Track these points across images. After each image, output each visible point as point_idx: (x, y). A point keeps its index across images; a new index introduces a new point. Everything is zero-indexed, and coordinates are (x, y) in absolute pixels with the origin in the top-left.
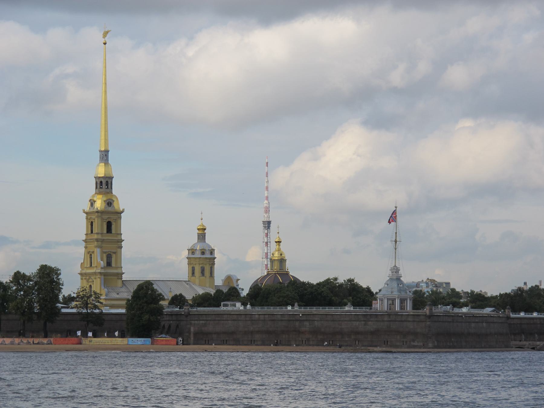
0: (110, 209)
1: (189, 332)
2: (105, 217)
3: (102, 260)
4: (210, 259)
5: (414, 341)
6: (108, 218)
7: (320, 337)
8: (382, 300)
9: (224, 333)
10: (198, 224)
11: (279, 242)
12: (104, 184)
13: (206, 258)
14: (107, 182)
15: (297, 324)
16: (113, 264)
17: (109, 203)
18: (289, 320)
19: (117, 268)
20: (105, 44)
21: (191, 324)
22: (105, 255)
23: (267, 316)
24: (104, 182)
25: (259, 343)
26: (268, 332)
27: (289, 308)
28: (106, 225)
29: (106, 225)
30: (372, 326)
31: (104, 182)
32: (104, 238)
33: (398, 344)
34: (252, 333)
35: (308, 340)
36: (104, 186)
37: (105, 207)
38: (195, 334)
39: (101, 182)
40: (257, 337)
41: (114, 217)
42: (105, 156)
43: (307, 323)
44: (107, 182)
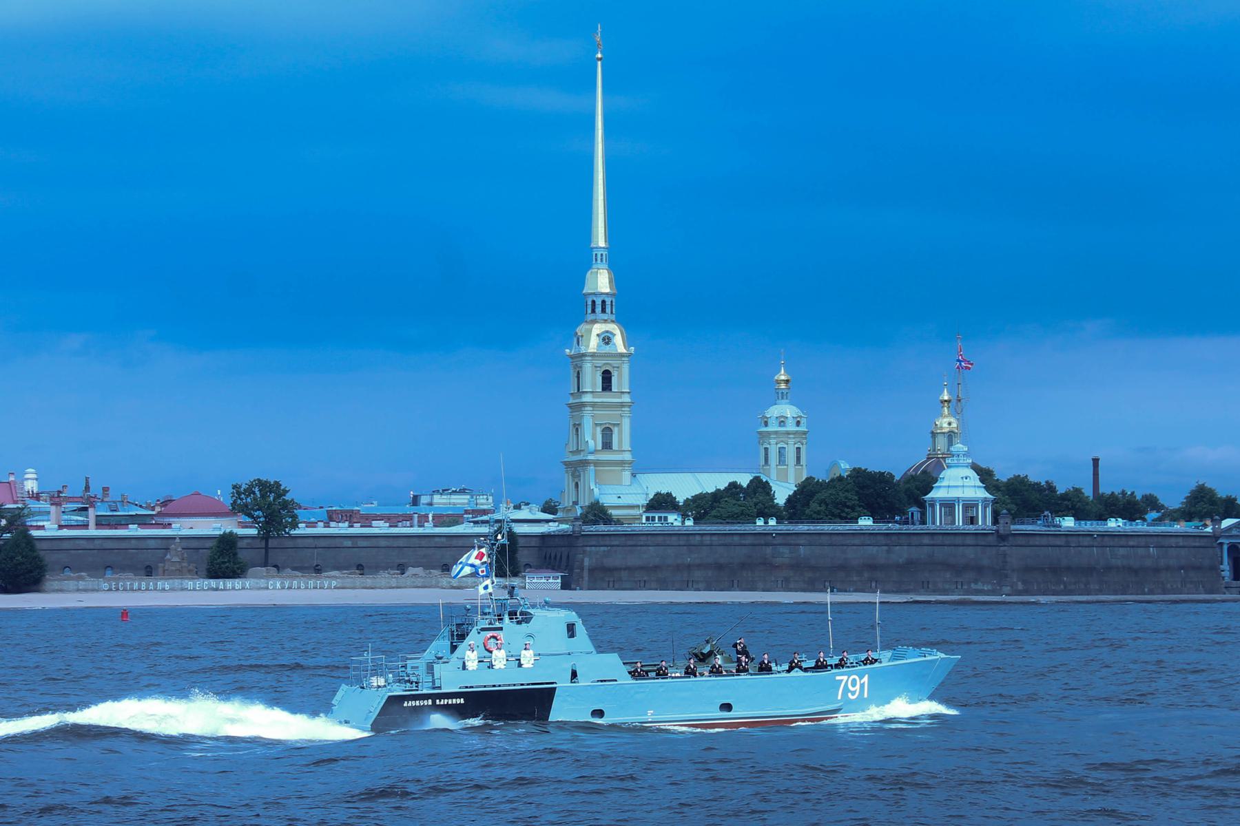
0: (607, 349)
1: (582, 569)
2: (600, 362)
3: (594, 438)
4: (795, 433)
5: (976, 582)
7: (808, 575)
8: (933, 506)
9: (642, 568)
11: (948, 401)
13: (788, 433)
14: (603, 302)
15: (769, 550)
16: (615, 447)
17: (607, 339)
18: (753, 545)
21: (584, 552)
22: (599, 430)
23: (714, 538)
24: (599, 302)
25: (700, 586)
26: (719, 567)
27: (760, 522)
30: (901, 554)
31: (599, 302)
33: (947, 586)
35: (787, 580)
36: (599, 309)
37: (599, 346)
39: (594, 302)
40: (698, 574)
41: (615, 363)
44: (603, 302)
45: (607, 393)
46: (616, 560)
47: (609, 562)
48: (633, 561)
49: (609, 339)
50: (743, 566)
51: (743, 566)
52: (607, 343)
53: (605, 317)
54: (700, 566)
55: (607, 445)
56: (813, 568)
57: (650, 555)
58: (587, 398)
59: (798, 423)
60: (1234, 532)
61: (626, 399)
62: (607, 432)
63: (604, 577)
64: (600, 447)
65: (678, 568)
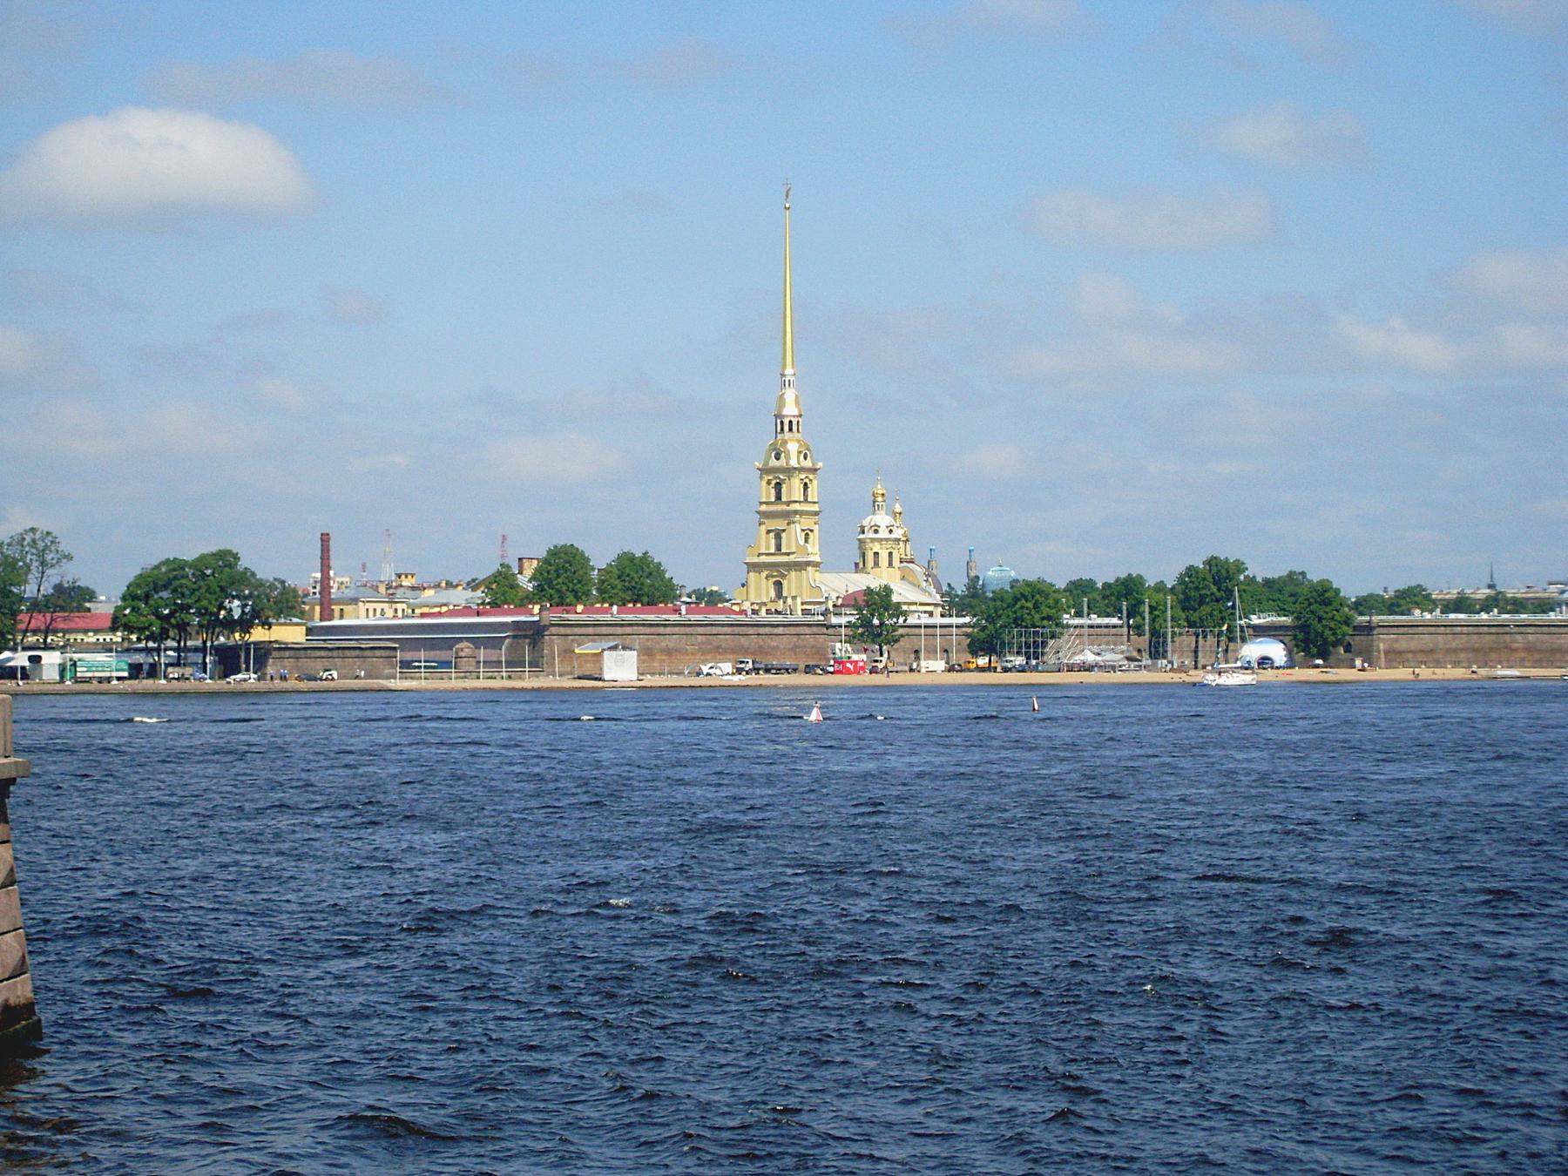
2: (803, 476)
7: (1537, 656)
9: (1422, 651)
26: (1475, 650)
34: (1455, 651)
35: (1523, 659)
38: (1387, 652)
40: (1462, 656)
43: (1519, 637)
46: (1404, 643)
47: (1396, 646)
48: (1413, 645)
50: (1491, 650)
51: (1491, 650)
54: (1463, 650)
56: (1539, 651)
57: (1426, 641)
58: (796, 507)
61: (816, 508)
63: (1395, 657)
65: (1448, 651)
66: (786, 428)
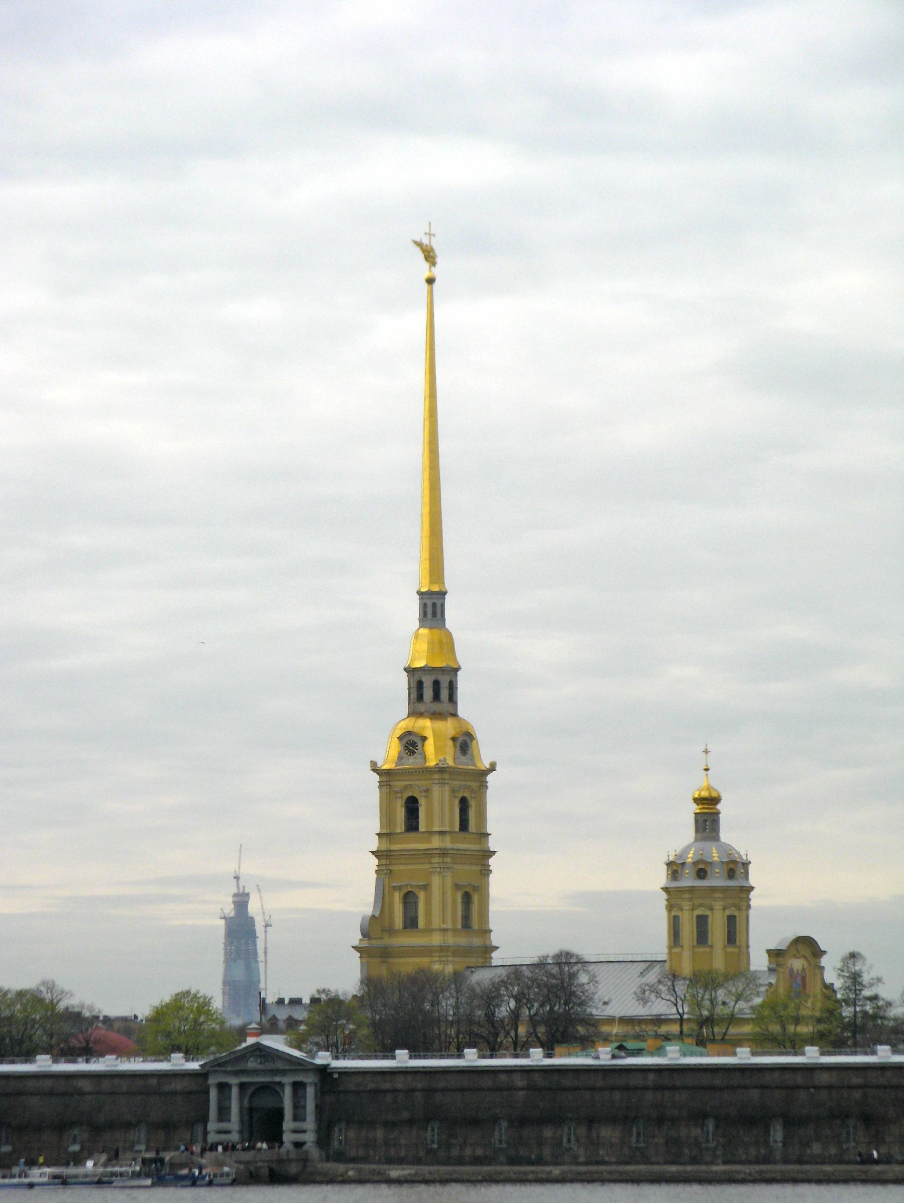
0: (411, 763)
2: (399, 784)
4: (692, 889)
6: (406, 787)
10: (697, 785)
12: (433, 689)
16: (421, 923)
19: (429, 931)
20: (430, 281)
22: (397, 897)
28: (434, 809)
29: (434, 809)
32: (395, 847)
37: (400, 758)
41: (423, 783)
42: (432, 607)
45: (412, 835)
49: (414, 744)
52: (412, 753)
53: (421, 707)
55: (411, 922)
59: (701, 874)
60: (252, 1064)
62: (409, 900)
64: (399, 922)
66: (428, 693)
